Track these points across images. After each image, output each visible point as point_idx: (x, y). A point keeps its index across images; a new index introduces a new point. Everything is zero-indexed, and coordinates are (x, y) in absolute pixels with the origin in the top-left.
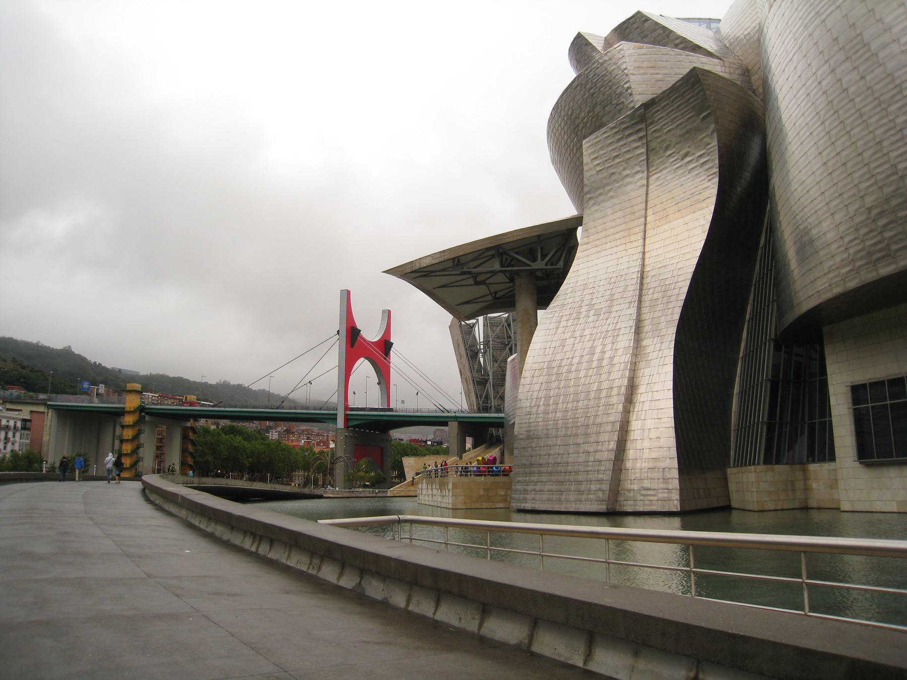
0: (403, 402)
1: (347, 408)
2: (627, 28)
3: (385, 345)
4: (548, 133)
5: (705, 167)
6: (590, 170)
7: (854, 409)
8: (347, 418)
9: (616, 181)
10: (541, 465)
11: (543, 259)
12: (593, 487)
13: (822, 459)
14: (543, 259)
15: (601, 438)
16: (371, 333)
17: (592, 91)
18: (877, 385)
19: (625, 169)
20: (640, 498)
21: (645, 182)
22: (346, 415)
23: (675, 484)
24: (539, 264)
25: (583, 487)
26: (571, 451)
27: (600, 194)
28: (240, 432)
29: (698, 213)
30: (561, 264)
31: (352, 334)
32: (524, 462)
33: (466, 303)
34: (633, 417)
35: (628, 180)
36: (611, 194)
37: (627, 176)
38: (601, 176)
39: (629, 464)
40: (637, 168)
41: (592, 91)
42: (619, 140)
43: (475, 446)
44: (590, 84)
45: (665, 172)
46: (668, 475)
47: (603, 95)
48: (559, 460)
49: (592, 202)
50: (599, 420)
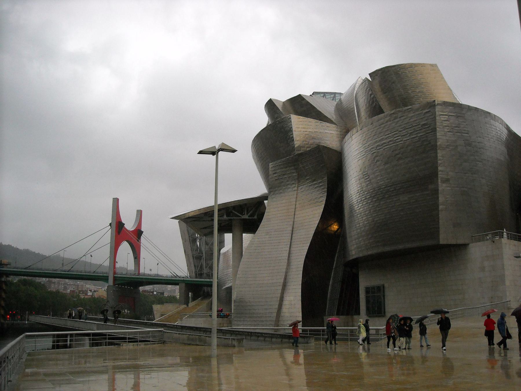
0: (151, 270)
1: (115, 273)
3: (138, 233)
4: (252, 146)
5: (322, 187)
7: (366, 297)
8: (115, 279)
9: (284, 186)
11: (247, 214)
13: (357, 315)
14: (247, 214)
16: (130, 225)
18: (373, 288)
19: (288, 181)
21: (296, 188)
22: (114, 277)
24: (246, 217)
28: (31, 284)
29: (318, 207)
30: (256, 217)
31: (118, 226)
33: (205, 228)
34: (285, 295)
35: (289, 186)
36: (281, 191)
37: (288, 184)
39: (282, 314)
40: (294, 182)
42: (286, 167)
43: (194, 299)
45: (305, 186)
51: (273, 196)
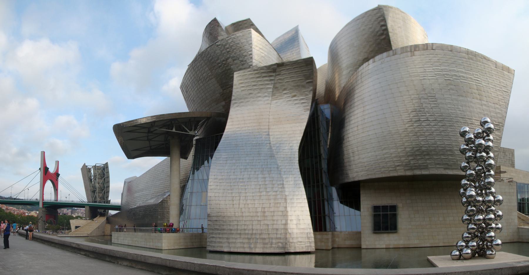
2: (241, 25)
6: (237, 88)
10: (231, 230)
12: (274, 241)
15: (275, 218)
17: (228, 50)
20: (297, 246)
23: (313, 240)
25: (267, 241)
26: (254, 224)
27: (242, 102)
32: (218, 227)
38: (244, 93)
41: (228, 50)
44: (228, 46)
46: (309, 236)
47: (235, 54)
48: (246, 228)
49: (236, 105)
50: (272, 210)
51: (238, 108)
